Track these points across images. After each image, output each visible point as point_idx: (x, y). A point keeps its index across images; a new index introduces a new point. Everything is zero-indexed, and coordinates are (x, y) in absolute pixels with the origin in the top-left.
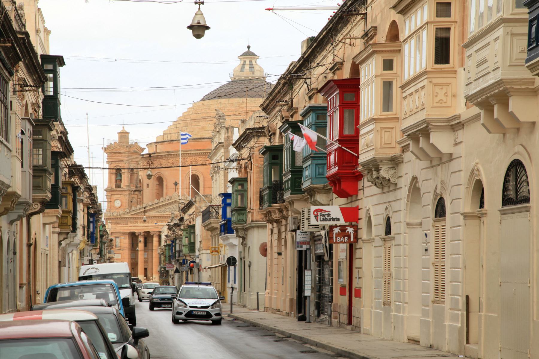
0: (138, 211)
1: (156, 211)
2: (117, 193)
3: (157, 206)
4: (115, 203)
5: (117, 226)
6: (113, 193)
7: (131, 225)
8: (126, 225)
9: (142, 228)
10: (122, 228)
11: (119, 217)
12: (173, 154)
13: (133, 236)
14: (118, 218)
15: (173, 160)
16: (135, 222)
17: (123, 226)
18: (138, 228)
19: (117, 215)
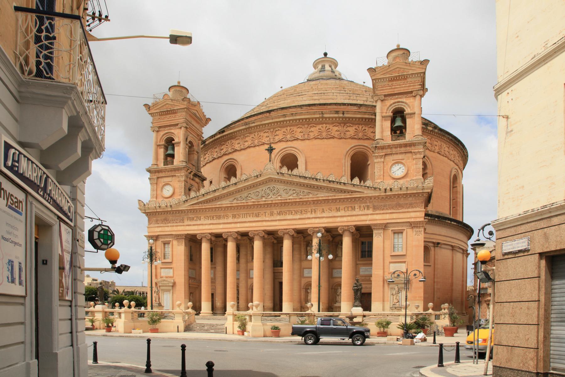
0: (201, 198)
1: (233, 198)
2: (167, 174)
3: (235, 188)
4: (164, 190)
5: (167, 225)
11: (170, 209)
12: (254, 127)
14: (167, 212)
15: (253, 136)
17: (176, 224)
19: (166, 206)
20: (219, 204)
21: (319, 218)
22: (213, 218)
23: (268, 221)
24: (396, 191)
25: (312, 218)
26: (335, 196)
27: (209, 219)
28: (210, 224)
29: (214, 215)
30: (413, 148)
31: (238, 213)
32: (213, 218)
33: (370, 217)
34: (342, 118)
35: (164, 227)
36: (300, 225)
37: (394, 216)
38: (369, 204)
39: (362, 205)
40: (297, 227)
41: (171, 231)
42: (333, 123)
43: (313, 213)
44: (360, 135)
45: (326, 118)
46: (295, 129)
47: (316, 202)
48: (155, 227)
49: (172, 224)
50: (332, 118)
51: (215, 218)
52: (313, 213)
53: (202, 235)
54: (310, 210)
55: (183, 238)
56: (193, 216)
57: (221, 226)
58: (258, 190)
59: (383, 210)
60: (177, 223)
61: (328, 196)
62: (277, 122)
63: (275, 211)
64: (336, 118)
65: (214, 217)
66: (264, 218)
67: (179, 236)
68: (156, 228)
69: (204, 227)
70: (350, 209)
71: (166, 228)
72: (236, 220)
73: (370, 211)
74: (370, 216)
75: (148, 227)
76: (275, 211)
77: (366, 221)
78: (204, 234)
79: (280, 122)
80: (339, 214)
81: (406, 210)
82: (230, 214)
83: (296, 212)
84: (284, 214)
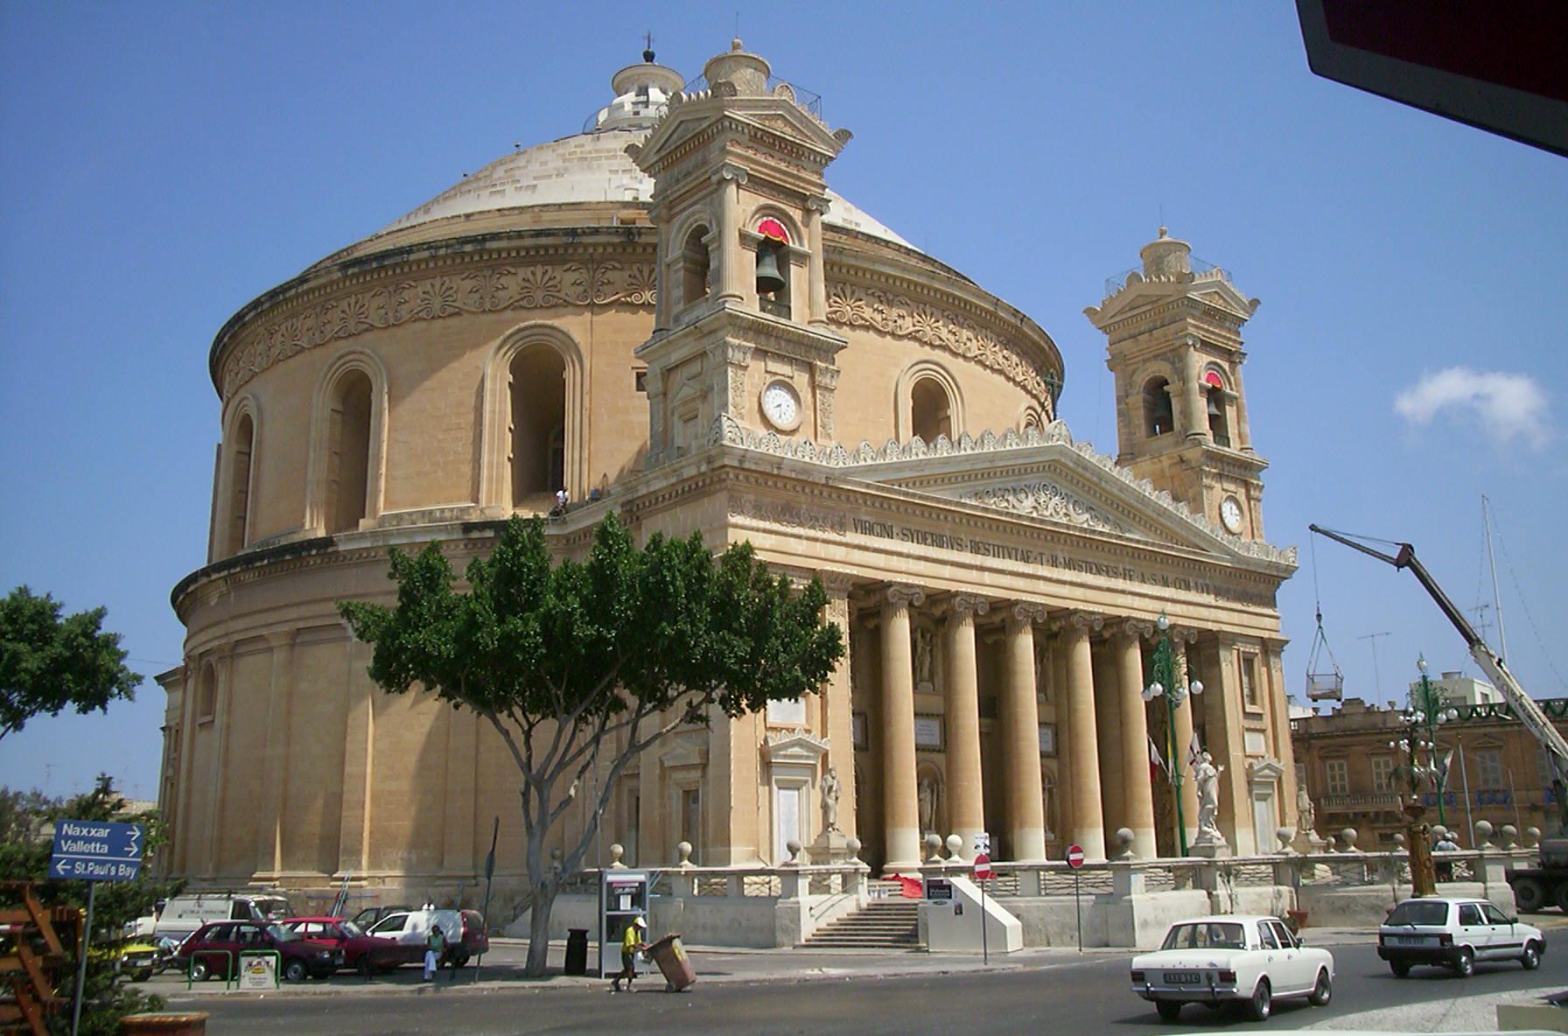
16: (877, 529)
27: (915, 540)
29: (927, 530)
33: (1213, 614)
35: (786, 535)
37: (1246, 619)
38: (1208, 582)
39: (1200, 581)
41: (806, 556)
43: (1127, 577)
48: (758, 530)
51: (929, 541)
52: (1127, 577)
54: (1122, 571)
65: (928, 535)
68: (761, 534)
71: (792, 539)
74: (1212, 610)
77: (1208, 620)
78: (912, 586)
84: (1077, 567)
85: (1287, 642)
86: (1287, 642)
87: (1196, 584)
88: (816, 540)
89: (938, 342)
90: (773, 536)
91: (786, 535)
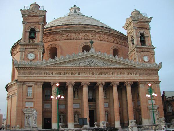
1: (72, 64)
6: (27, 47)
7: (46, 75)
8: (40, 76)
9: (57, 78)
10: (36, 78)
13: (47, 86)
18: (53, 78)
20: (65, 66)
21: (116, 77)
22: (60, 73)
23: (91, 77)
24: (149, 67)
25: (113, 77)
26: (124, 67)
28: (59, 77)
30: (150, 50)
31: (75, 72)
32: (60, 73)
33: (138, 78)
34: (109, 33)
35: (29, 77)
36: (108, 80)
37: (148, 78)
39: (134, 72)
40: (106, 81)
42: (105, 35)
43: (113, 74)
44: (115, 42)
45: (103, 32)
46: (89, 34)
47: (115, 69)
48: (23, 76)
49: (34, 76)
50: (105, 32)
52: (113, 74)
53: (54, 83)
55: (42, 84)
56: (48, 72)
57: (65, 78)
58: (85, 61)
59: (143, 75)
60: (38, 75)
61: (121, 67)
62: (81, 30)
63: (95, 72)
64: (107, 33)
66: (89, 76)
67: (39, 83)
69: (55, 78)
70: (129, 74)
72: (73, 76)
73: (138, 76)
74: (138, 78)
75: (18, 76)
76: (95, 72)
79: (82, 30)
80: (125, 76)
81: (152, 76)
82: (70, 72)
83: (105, 74)
85: (160, 81)
86: (160, 81)
87: (134, 73)
88: (36, 77)
89: (88, 39)
90: (27, 77)
91: (29, 77)
